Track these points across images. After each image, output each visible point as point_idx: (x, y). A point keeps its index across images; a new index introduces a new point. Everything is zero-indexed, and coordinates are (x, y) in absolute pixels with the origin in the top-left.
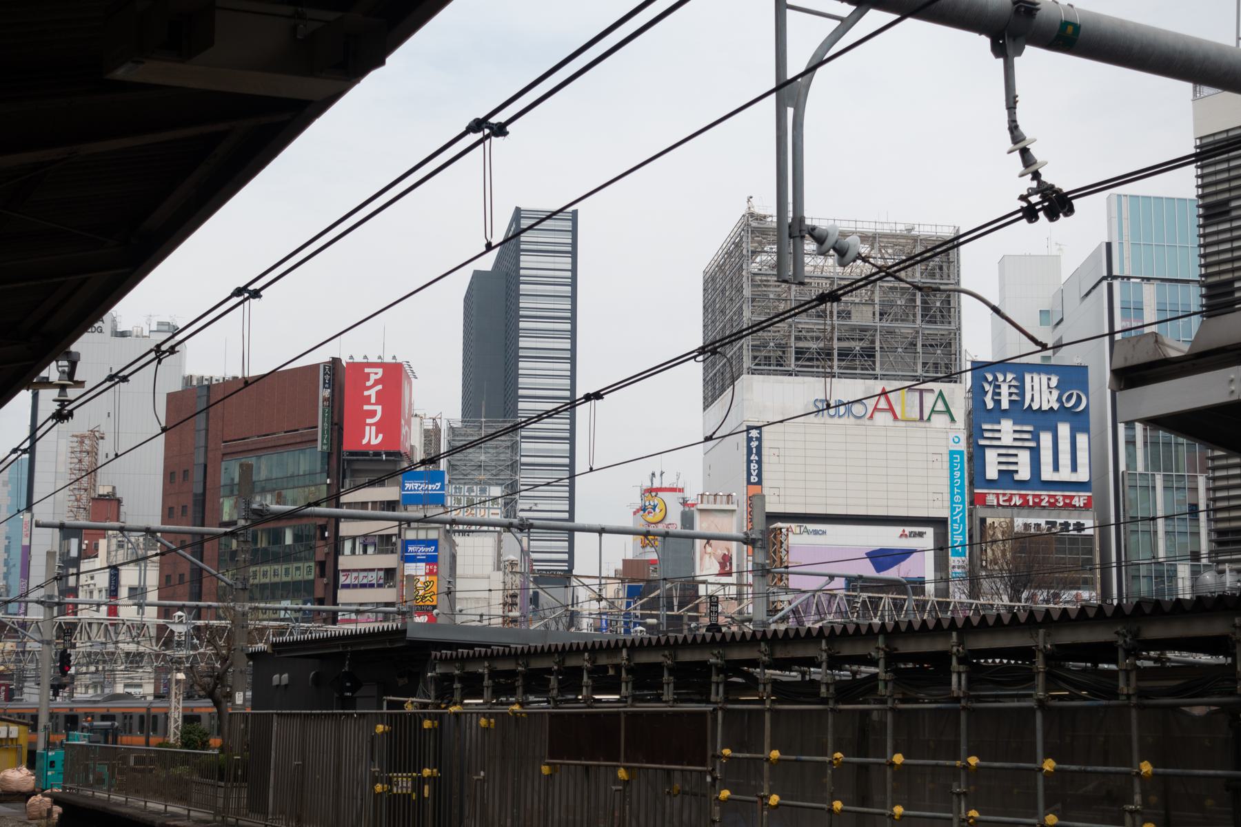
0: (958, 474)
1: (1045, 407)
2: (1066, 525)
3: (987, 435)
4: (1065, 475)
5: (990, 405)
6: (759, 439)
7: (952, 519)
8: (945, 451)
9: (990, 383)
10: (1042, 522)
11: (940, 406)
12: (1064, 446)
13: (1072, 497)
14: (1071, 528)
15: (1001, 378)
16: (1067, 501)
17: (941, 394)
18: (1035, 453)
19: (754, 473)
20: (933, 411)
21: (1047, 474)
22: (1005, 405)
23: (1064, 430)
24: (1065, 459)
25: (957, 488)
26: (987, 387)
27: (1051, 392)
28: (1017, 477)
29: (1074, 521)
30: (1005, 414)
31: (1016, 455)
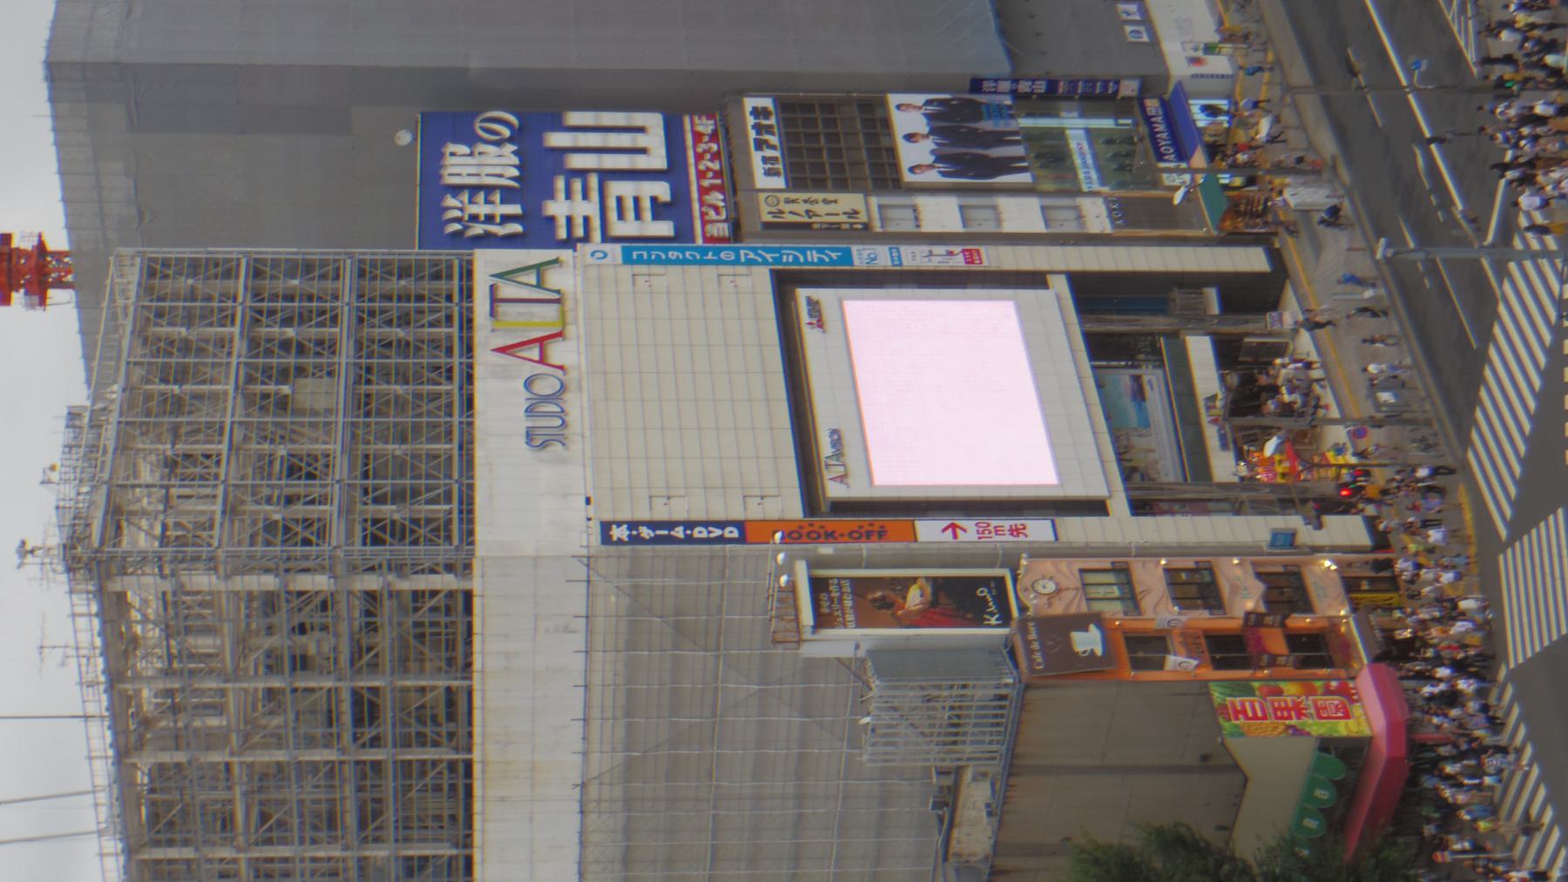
0: (673, 255)
6: (633, 525)
7: (771, 264)
8: (627, 271)
19: (717, 532)
23: (556, 139)
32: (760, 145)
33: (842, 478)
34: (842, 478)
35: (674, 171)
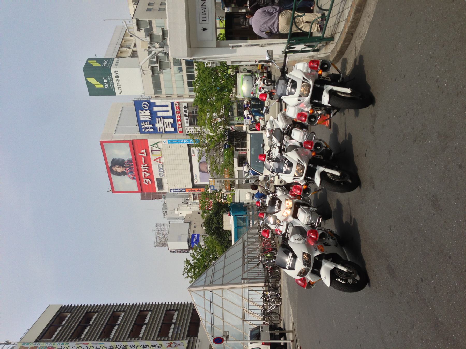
1: (149, 114)
2: (185, 111)
3: (161, 131)
4: (169, 108)
5: (152, 130)
6: (173, 189)
8: (168, 145)
9: (145, 130)
10: (185, 118)
11: (156, 145)
12: (160, 109)
13: (176, 107)
14: (186, 110)
15: (143, 127)
16: (177, 108)
17: (151, 145)
18: (164, 117)
19: (182, 190)
20: (157, 148)
21: (170, 114)
22: (151, 126)
23: (155, 109)
24: (164, 109)
25: (179, 141)
26: (147, 130)
28: (173, 122)
29: (184, 109)
30: (154, 125)
31: (166, 123)
32: (185, 115)
33: (196, 182)
34: (196, 182)
35: (173, 117)
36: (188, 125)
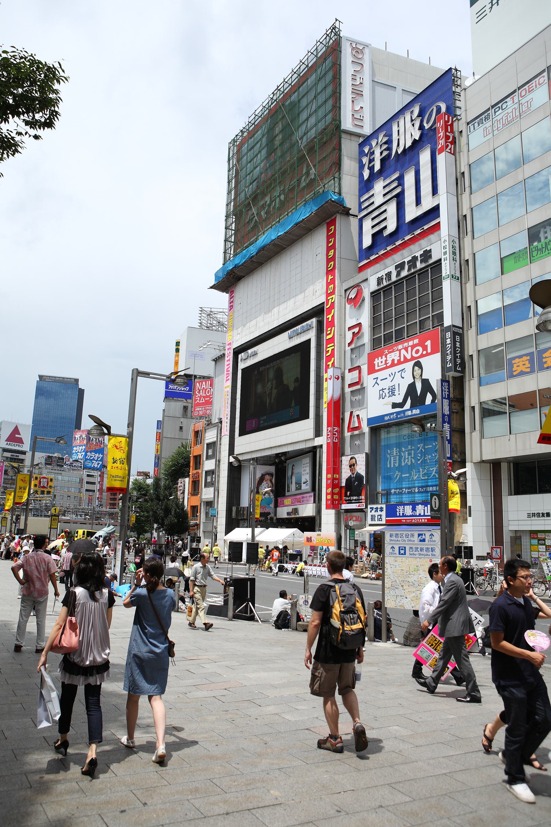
27: (413, 125)
28: (386, 233)
32: (401, 267)
36: (372, 285)
